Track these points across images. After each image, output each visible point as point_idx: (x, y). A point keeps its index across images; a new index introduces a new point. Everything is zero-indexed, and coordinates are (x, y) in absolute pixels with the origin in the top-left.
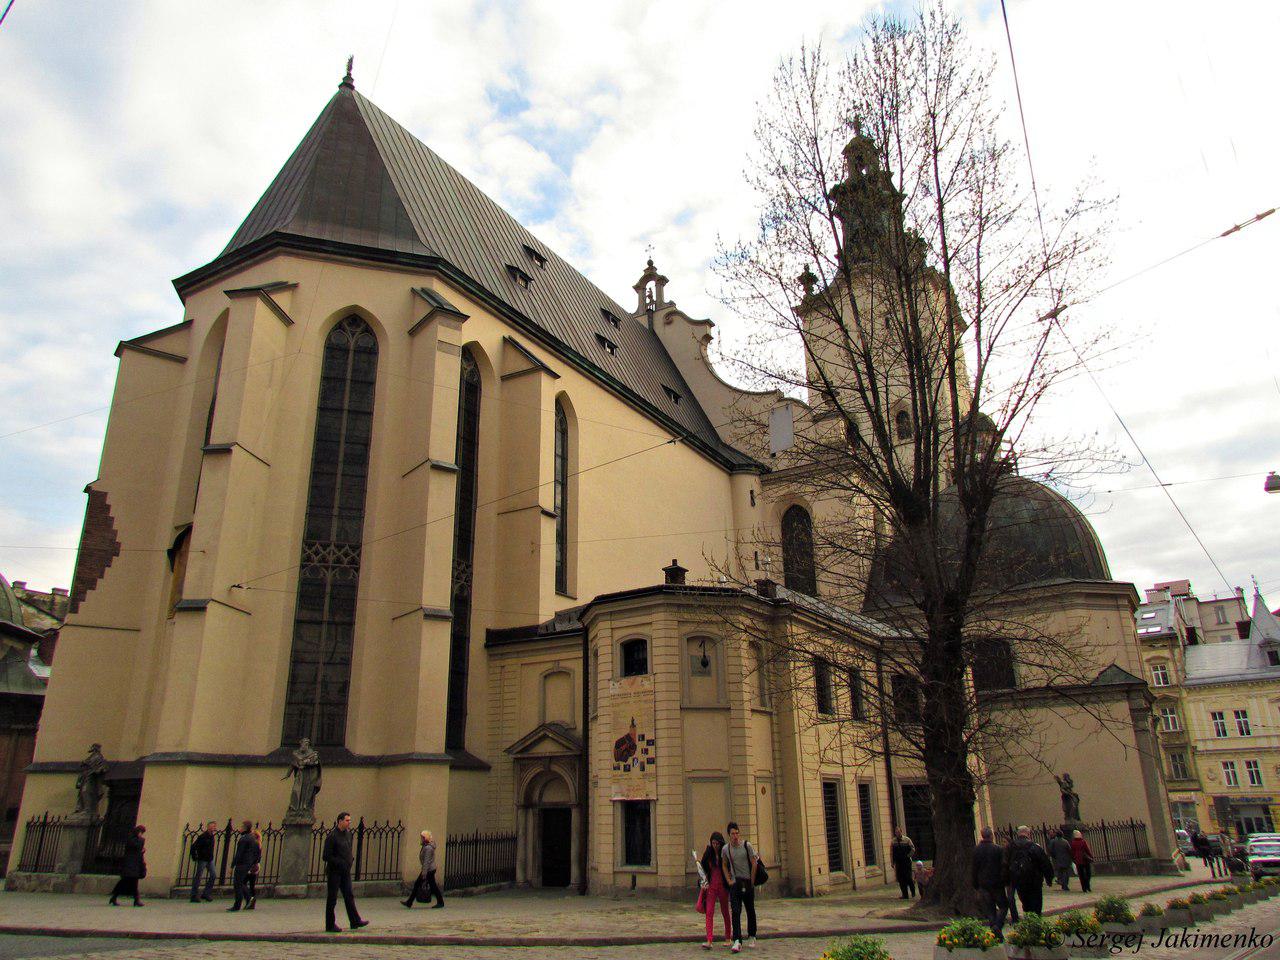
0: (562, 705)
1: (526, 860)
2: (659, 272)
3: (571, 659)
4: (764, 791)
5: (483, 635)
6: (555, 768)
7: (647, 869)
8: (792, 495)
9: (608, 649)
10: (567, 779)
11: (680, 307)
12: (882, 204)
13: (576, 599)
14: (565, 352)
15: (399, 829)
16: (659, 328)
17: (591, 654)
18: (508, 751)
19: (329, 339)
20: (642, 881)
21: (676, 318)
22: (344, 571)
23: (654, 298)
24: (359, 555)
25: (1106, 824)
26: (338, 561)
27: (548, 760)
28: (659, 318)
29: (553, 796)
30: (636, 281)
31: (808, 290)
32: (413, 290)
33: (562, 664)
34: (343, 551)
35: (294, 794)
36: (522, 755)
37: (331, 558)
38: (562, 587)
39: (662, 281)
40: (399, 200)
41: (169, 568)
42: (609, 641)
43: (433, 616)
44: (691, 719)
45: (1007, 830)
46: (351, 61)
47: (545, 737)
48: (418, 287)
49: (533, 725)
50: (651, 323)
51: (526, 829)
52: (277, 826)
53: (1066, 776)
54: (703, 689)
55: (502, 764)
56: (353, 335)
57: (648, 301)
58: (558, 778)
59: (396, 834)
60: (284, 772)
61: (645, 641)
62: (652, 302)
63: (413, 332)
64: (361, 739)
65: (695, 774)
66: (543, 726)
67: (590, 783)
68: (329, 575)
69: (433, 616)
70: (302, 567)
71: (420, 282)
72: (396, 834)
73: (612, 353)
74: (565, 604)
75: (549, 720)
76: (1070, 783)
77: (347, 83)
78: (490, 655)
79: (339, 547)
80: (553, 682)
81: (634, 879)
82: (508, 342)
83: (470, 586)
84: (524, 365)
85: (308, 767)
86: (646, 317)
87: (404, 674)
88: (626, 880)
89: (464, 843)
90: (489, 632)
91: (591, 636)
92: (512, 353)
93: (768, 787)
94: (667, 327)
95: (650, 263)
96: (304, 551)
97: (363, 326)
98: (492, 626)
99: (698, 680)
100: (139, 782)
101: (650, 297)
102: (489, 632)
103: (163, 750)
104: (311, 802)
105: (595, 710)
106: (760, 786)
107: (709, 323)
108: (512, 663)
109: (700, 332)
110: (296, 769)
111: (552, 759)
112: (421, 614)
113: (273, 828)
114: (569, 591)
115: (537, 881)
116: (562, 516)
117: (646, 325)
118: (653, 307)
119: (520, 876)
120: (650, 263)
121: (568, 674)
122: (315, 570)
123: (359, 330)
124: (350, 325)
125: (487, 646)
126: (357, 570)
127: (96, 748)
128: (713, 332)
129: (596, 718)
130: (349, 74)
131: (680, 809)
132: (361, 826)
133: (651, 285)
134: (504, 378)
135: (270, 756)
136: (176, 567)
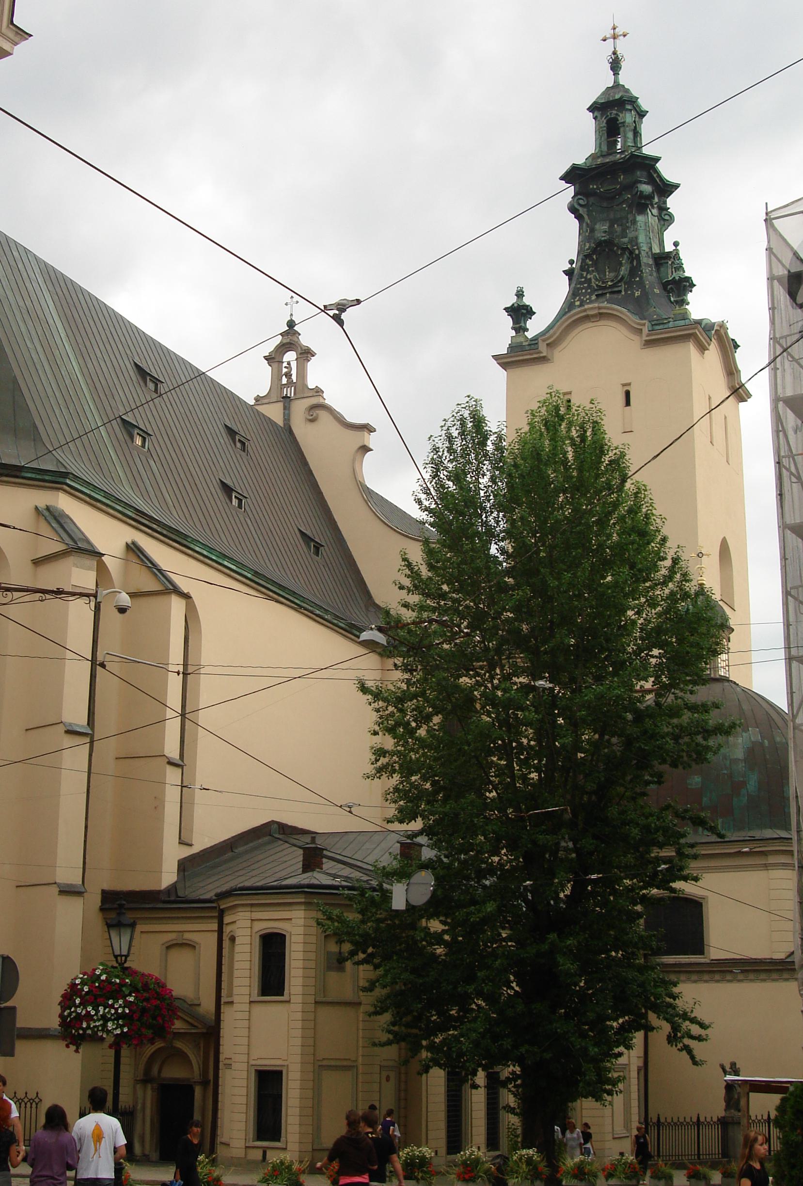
1: (143, 1134)
2: (305, 340)
6: (179, 1044)
10: (192, 1057)
11: (330, 399)
12: (642, 204)
13: (191, 845)
14: (192, 546)
15: (37, 1100)
17: (225, 938)
21: (322, 414)
23: (294, 378)
28: (299, 408)
29: (174, 1072)
30: (270, 347)
31: (519, 328)
32: (36, 508)
33: (187, 936)
39: (306, 354)
40: (15, 381)
43: (67, 891)
44: (325, 1013)
45: (765, 1117)
48: (42, 505)
50: (287, 418)
51: (144, 1104)
57: (284, 380)
59: (34, 1105)
61: (285, 936)
62: (290, 383)
65: (325, 1063)
67: (221, 1063)
71: (42, 498)
72: (34, 1105)
73: (240, 506)
80: (174, 954)
82: (133, 549)
84: (152, 585)
86: (280, 406)
88: (257, 1155)
91: (227, 919)
93: (392, 1075)
94: (311, 426)
95: (291, 324)
98: (106, 887)
99: (333, 976)
101: (288, 375)
106: (384, 1074)
107: (367, 428)
112: (55, 890)
115: (155, 1156)
117: (280, 423)
118: (290, 392)
120: (291, 324)
121: (194, 947)
125: (102, 909)
128: (372, 440)
133: (290, 356)
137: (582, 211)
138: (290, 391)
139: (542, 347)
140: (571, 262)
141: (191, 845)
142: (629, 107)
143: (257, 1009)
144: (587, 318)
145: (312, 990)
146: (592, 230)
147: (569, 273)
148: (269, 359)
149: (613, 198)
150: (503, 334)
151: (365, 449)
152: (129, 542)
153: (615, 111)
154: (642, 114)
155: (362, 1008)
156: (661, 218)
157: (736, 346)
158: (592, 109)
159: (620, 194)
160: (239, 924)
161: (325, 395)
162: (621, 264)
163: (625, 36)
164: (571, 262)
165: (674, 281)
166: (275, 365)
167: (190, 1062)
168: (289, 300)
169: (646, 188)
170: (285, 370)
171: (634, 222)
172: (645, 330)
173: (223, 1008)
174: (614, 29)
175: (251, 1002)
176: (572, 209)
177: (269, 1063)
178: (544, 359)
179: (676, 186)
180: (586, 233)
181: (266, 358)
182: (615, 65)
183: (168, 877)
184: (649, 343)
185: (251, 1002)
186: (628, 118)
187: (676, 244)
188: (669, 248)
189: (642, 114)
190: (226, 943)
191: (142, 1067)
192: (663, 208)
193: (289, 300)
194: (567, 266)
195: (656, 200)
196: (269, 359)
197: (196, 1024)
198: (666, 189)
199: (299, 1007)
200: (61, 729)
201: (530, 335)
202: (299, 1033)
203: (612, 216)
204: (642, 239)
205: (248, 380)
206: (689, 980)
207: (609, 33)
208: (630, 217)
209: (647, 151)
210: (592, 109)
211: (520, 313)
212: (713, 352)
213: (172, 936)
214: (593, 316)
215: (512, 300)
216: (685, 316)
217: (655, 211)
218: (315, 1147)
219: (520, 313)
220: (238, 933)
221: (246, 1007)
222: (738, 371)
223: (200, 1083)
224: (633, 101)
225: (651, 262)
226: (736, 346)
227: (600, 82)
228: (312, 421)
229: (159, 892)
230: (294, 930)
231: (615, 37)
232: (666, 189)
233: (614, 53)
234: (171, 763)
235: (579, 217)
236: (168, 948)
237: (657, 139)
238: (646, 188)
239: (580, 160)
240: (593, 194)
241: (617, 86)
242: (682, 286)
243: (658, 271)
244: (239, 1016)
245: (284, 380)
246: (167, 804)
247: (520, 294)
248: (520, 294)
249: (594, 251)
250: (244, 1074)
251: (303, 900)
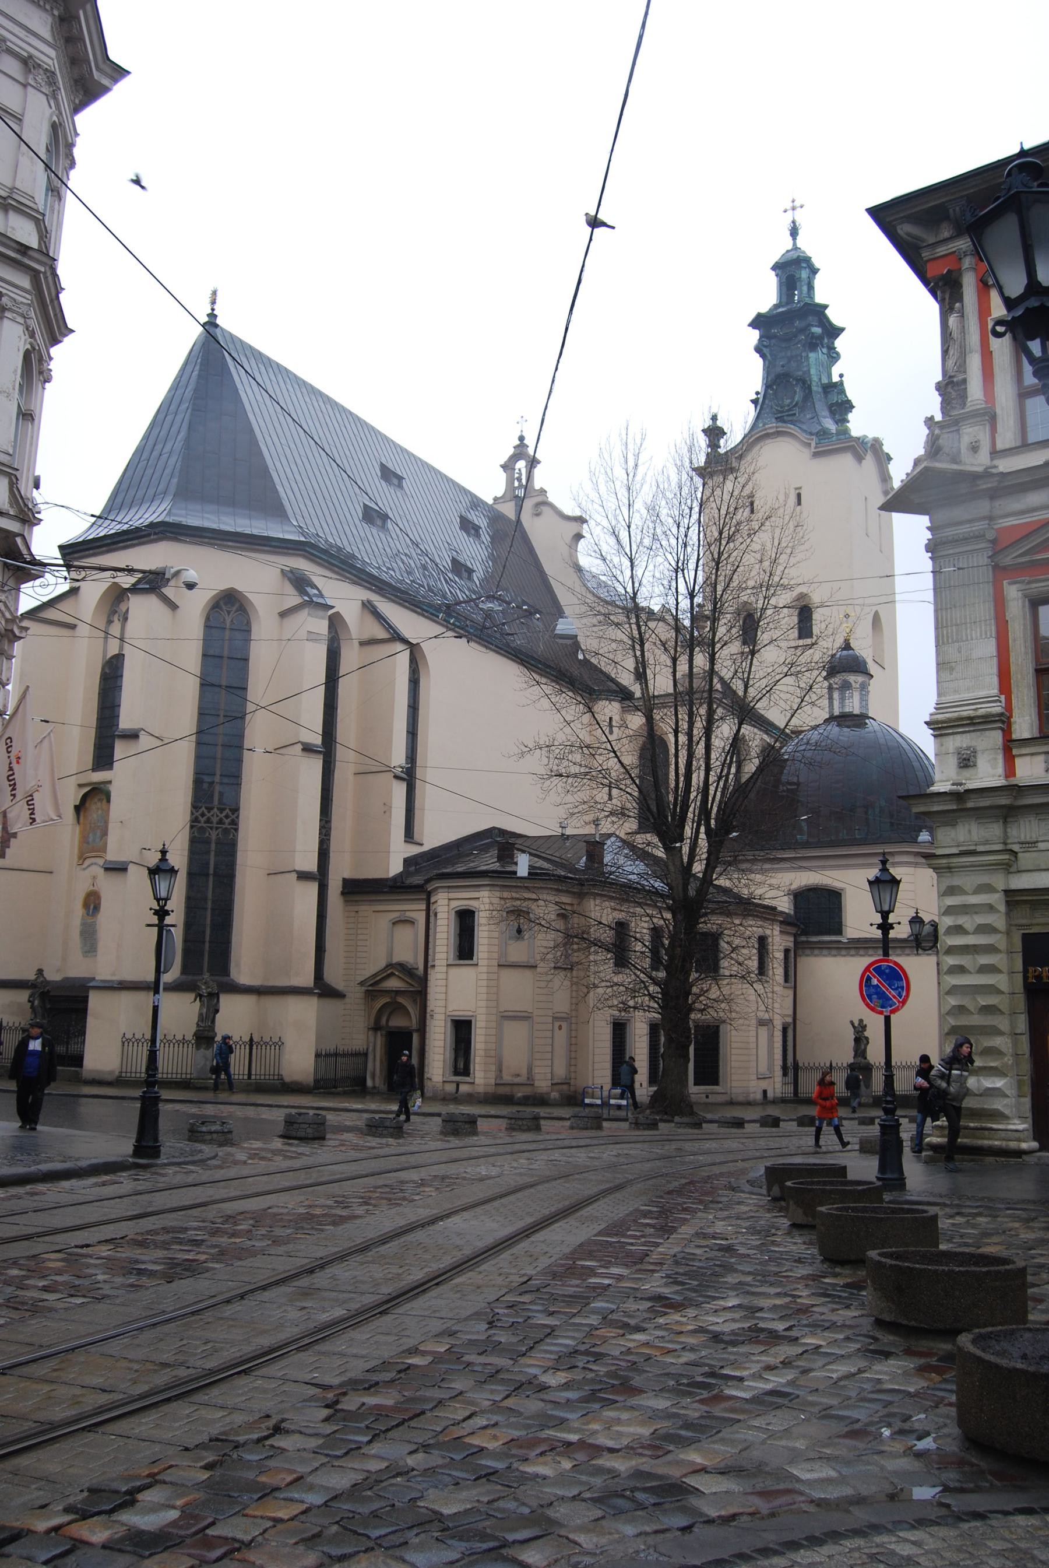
0: (406, 948)
3: (416, 910)
4: (560, 1028)
5: (340, 883)
6: (400, 1000)
7: (467, 1079)
9: (445, 915)
11: (552, 498)
12: (813, 344)
13: (422, 845)
16: (527, 519)
18: (362, 983)
19: (208, 619)
20: (464, 1088)
22: (226, 831)
24: (238, 817)
25: (834, 1065)
26: (221, 822)
27: (393, 994)
28: (528, 504)
29: (398, 1022)
30: (504, 458)
31: (714, 445)
33: (408, 914)
34: (224, 814)
35: (201, 1015)
36: (372, 988)
37: (215, 820)
38: (409, 835)
41: (76, 822)
42: (446, 909)
44: (507, 974)
46: (214, 293)
47: (392, 974)
49: (382, 964)
52: (189, 1037)
53: (861, 1021)
54: (517, 952)
55: (355, 995)
56: (229, 612)
57: (516, 484)
58: (402, 1008)
60: (191, 996)
62: (520, 486)
63: (283, 615)
64: (243, 971)
65: (506, 1014)
66: (390, 966)
68: (214, 835)
69: (303, 876)
74: (414, 850)
75: (394, 961)
76: (864, 1028)
77: (211, 325)
78: (346, 901)
79: (221, 810)
81: (458, 1086)
83: (329, 840)
84: (383, 634)
85: (211, 995)
86: (512, 504)
87: (273, 918)
89: (327, 1055)
90: (344, 880)
91: (432, 900)
92: (370, 620)
93: (564, 1025)
94: (536, 519)
96: (192, 814)
97: (237, 605)
98: (347, 876)
100: (85, 1000)
101: (519, 479)
102: (344, 880)
103: (103, 978)
104: (213, 1021)
105: (434, 961)
106: (557, 1024)
107: (581, 520)
108: (366, 909)
109: (573, 528)
110: (201, 996)
111: (398, 992)
112: (294, 876)
113: (187, 1038)
114: (416, 837)
116: (409, 776)
117: (512, 515)
118: (521, 493)
119: (369, 1083)
122: (202, 830)
123: (234, 609)
124: (225, 604)
125: (343, 893)
126: (236, 830)
127: (40, 972)
129: (434, 966)
130: (213, 310)
131: (493, 1039)
132: (251, 1040)
133: (521, 465)
134: (362, 644)
136: (81, 818)
137: (766, 351)
138: (523, 493)
140: (757, 393)
141: (422, 845)
142: (804, 265)
143: (453, 971)
144: (768, 436)
145: (495, 955)
147: (755, 402)
148: (504, 467)
149: (789, 340)
151: (579, 537)
152: (365, 599)
154: (814, 271)
155: (538, 970)
156: (829, 356)
157: (889, 459)
158: (774, 268)
159: (796, 336)
160: (440, 902)
161: (548, 495)
162: (795, 392)
163: (801, 207)
164: (757, 393)
165: (837, 404)
166: (509, 471)
167: (408, 1014)
168: (520, 420)
169: (817, 330)
170: (516, 475)
172: (813, 444)
174: (793, 201)
175: (448, 965)
176: (758, 350)
177: (462, 1014)
179: (842, 330)
180: (768, 369)
181: (502, 466)
182: (794, 232)
183: (395, 868)
184: (816, 455)
185: (448, 965)
186: (804, 274)
187: (841, 376)
188: (835, 379)
189: (814, 271)
190: (432, 919)
191: (372, 1020)
192: (831, 348)
193: (520, 420)
194: (754, 397)
195: (826, 341)
196: (504, 467)
198: (835, 332)
199: (484, 969)
200: (300, 747)
201: (722, 451)
202: (484, 990)
203: (789, 354)
204: (813, 371)
205: (489, 485)
206: (830, 955)
207: (789, 205)
208: (804, 354)
209: (819, 298)
210: (774, 268)
211: (714, 433)
212: (869, 461)
213: (397, 914)
214: (772, 434)
215: (708, 423)
216: (846, 432)
217: (825, 350)
218: (498, 1082)
219: (714, 433)
220: (439, 909)
221: (444, 969)
222: (890, 478)
223: (418, 1030)
224: (808, 260)
225: (820, 390)
226: (889, 459)
227: (780, 247)
228: (538, 515)
229: (387, 880)
230: (482, 907)
231: (794, 209)
232: (835, 332)
233: (794, 222)
234: (396, 777)
235: (763, 356)
237: (824, 291)
238: (817, 330)
239: (764, 309)
240: (775, 337)
241: (795, 248)
242: (842, 407)
243: (826, 397)
244: (439, 976)
245: (516, 484)
246: (393, 810)
247: (714, 418)
248: (714, 418)
249: (774, 382)
250: (442, 1023)
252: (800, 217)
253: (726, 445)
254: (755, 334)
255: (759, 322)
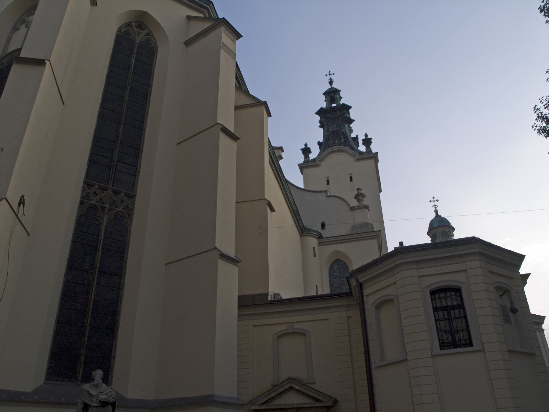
8: (337, 252)
33: (297, 326)
63: (188, 43)
70: (82, 203)
96: (83, 191)
135: (36, 391)
139: (317, 161)
144: (333, 152)
146: (328, 129)
147: (319, 143)
150: (301, 159)
153: (332, 94)
171: (344, 126)
172: (357, 155)
173: (375, 374)
175: (433, 356)
178: (318, 166)
179: (354, 121)
182: (331, 82)
184: (358, 160)
197: (320, 398)
200: (219, 127)
201: (310, 159)
207: (328, 73)
210: (324, 94)
211: (306, 151)
213: (284, 327)
215: (303, 147)
219: (306, 151)
231: (330, 75)
233: (331, 79)
236: (279, 337)
247: (306, 145)
248: (306, 145)
251: (478, 250)
252: (332, 77)
253: (312, 156)
254: (318, 118)
255: (321, 112)
